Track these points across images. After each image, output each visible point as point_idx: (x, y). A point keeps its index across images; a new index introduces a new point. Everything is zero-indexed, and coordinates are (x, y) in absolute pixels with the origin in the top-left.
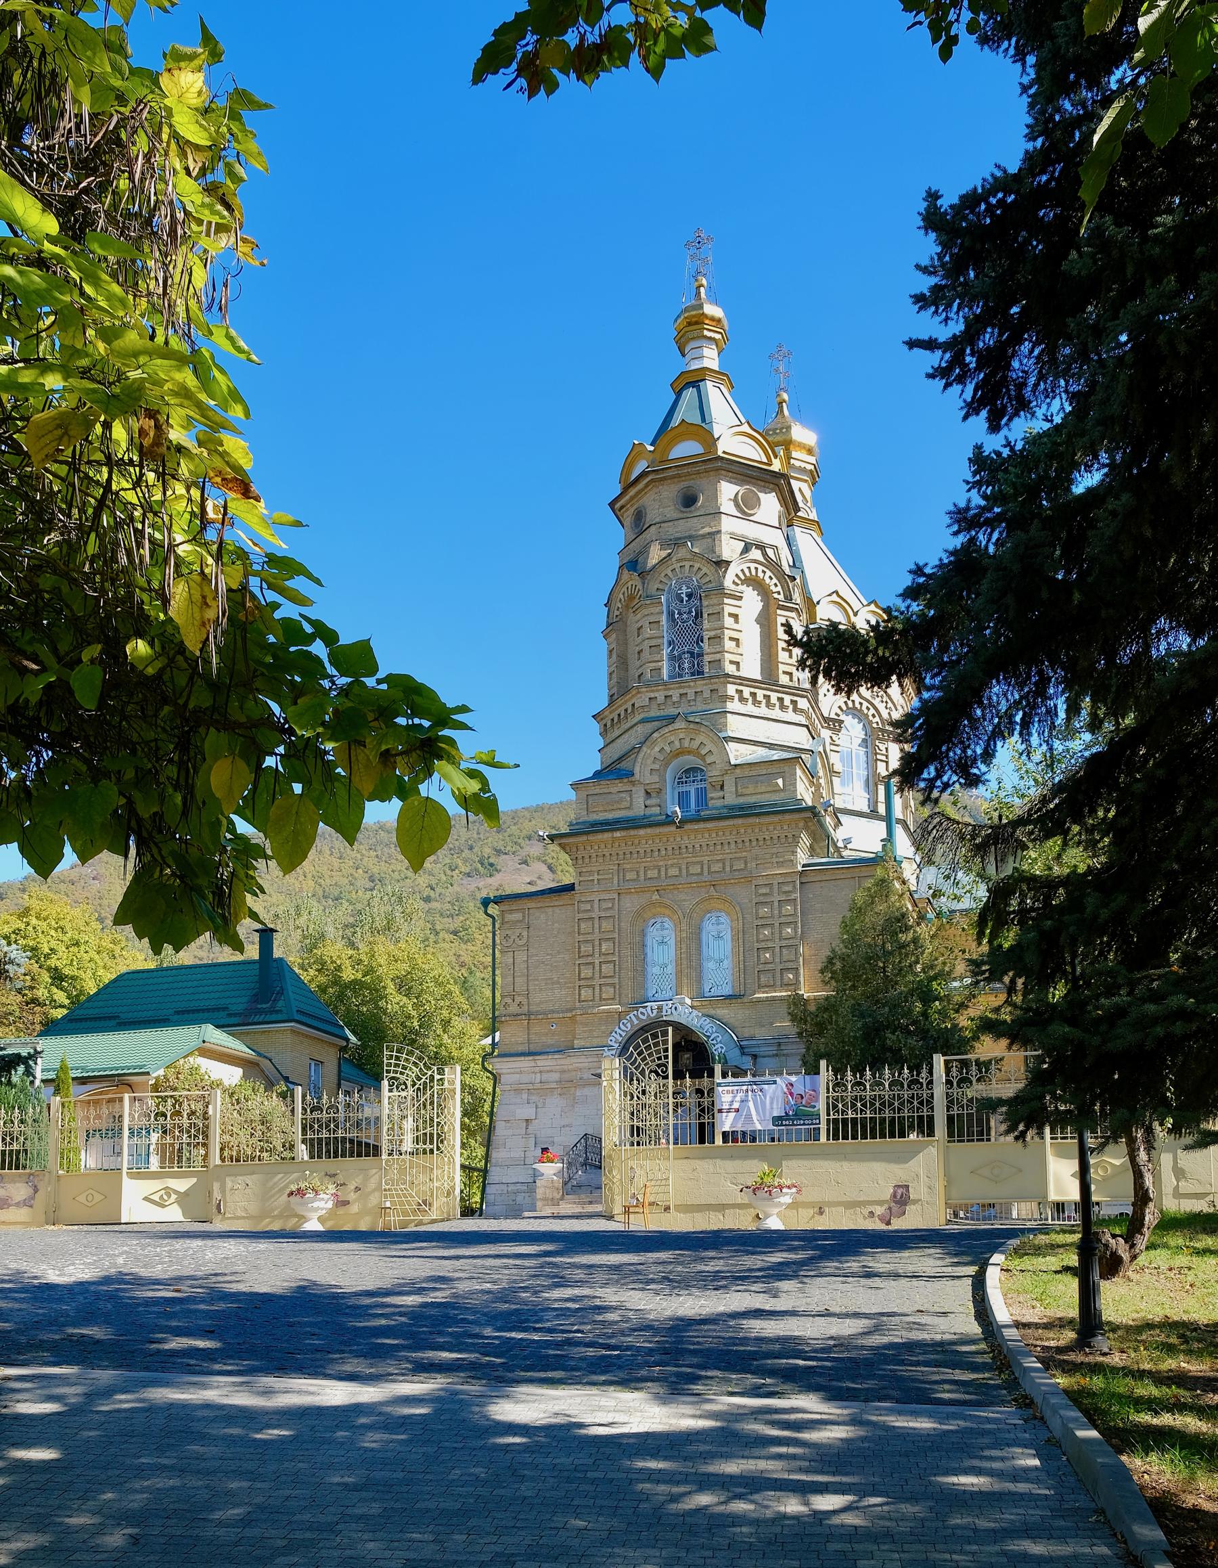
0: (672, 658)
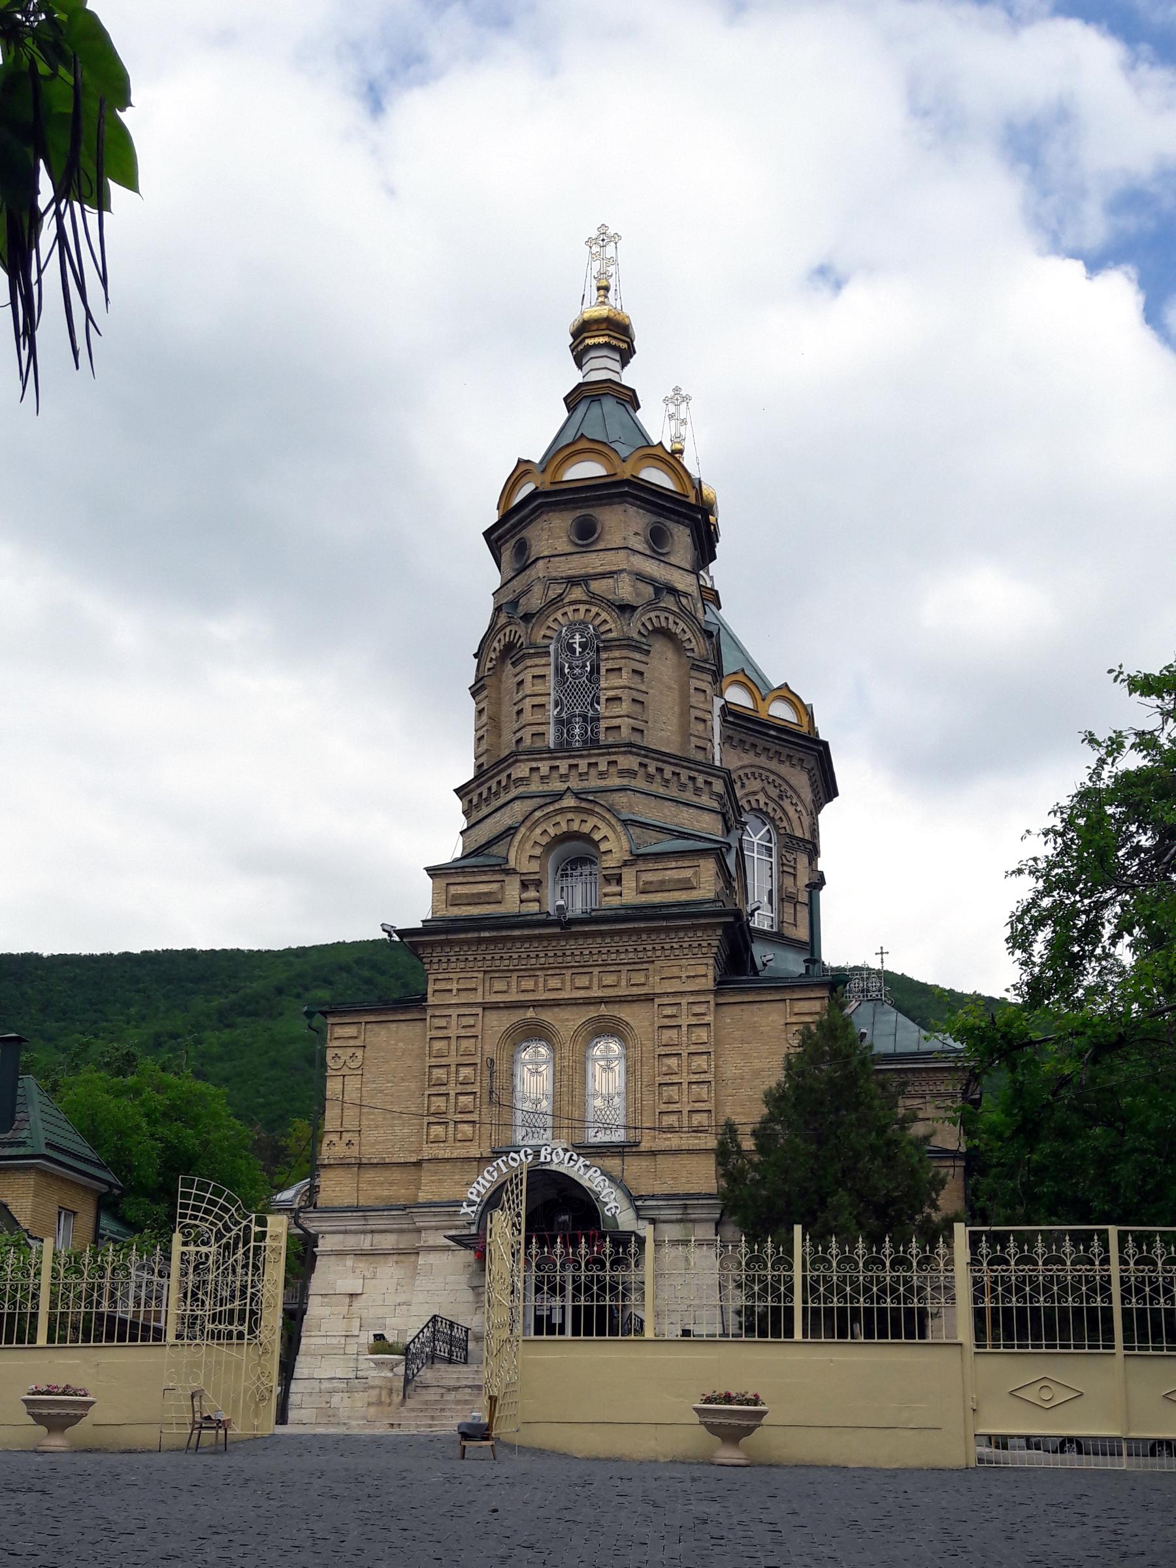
0: (560, 722)
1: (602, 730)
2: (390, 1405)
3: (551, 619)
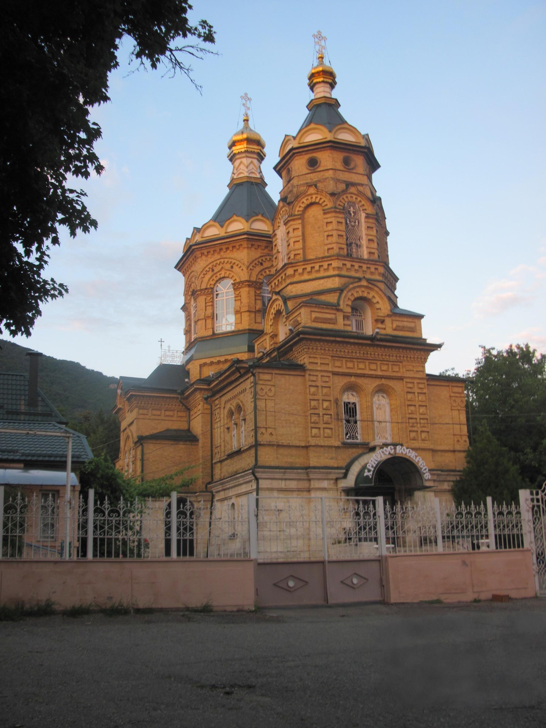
3: (341, 198)
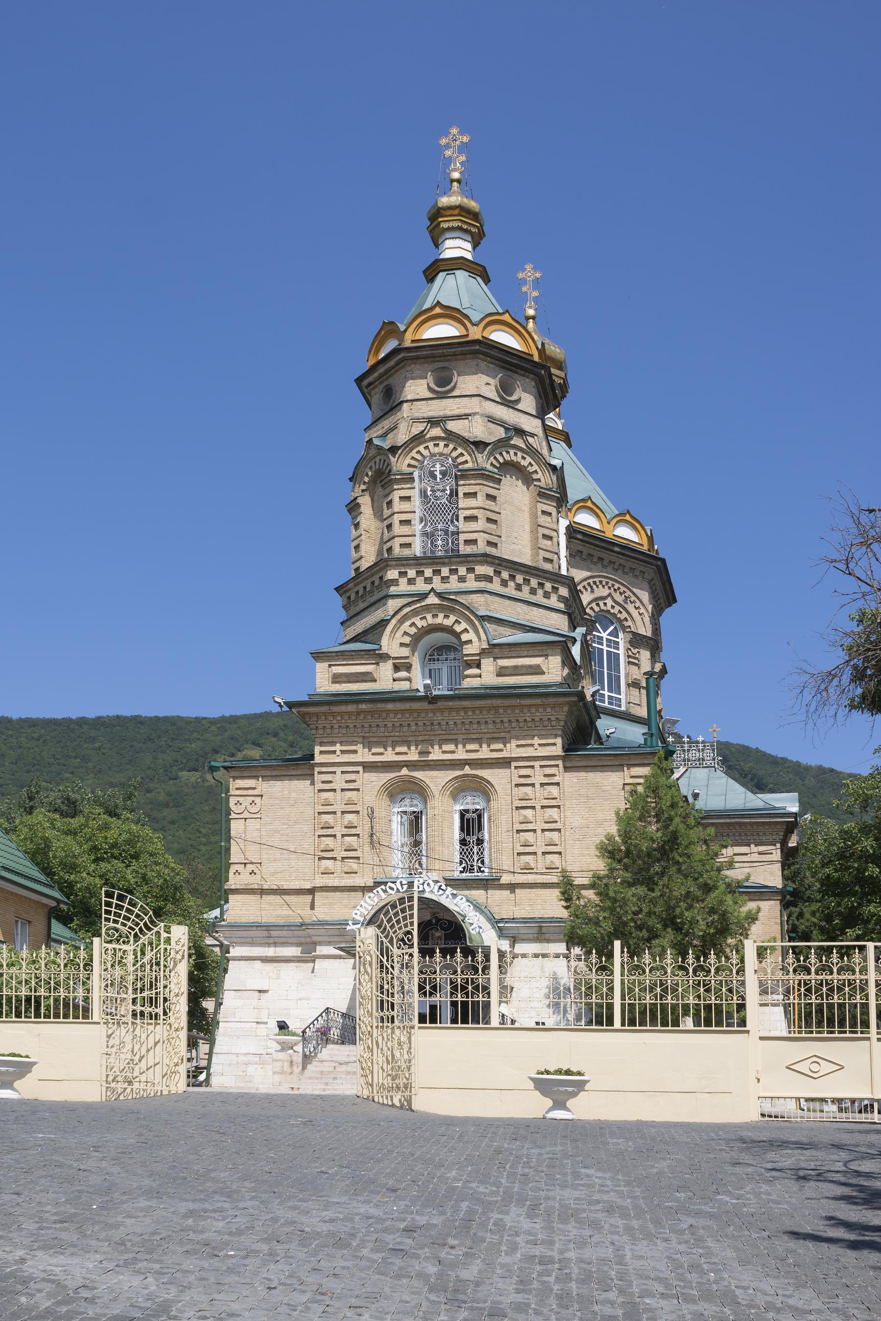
0: (425, 534)
1: (461, 542)
2: (291, 1073)
3: (415, 451)
